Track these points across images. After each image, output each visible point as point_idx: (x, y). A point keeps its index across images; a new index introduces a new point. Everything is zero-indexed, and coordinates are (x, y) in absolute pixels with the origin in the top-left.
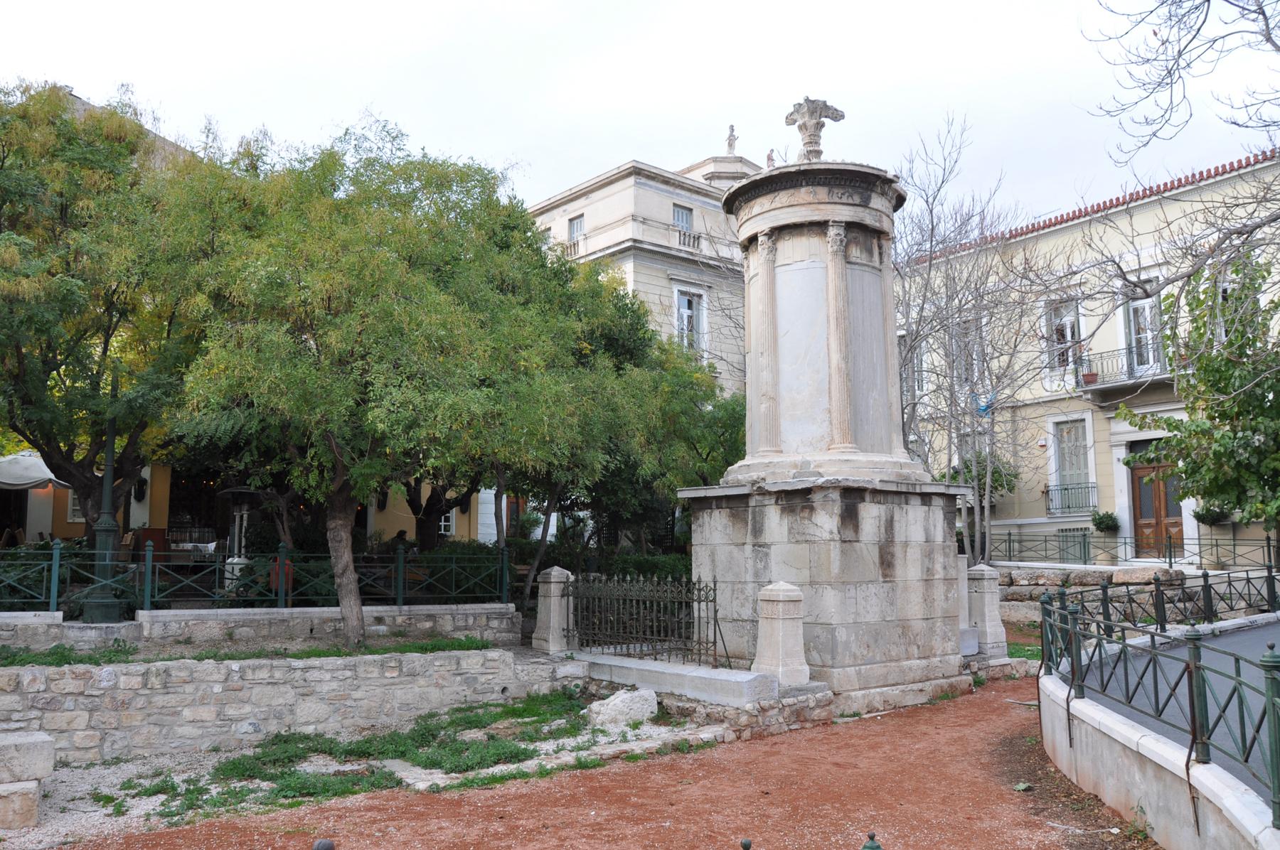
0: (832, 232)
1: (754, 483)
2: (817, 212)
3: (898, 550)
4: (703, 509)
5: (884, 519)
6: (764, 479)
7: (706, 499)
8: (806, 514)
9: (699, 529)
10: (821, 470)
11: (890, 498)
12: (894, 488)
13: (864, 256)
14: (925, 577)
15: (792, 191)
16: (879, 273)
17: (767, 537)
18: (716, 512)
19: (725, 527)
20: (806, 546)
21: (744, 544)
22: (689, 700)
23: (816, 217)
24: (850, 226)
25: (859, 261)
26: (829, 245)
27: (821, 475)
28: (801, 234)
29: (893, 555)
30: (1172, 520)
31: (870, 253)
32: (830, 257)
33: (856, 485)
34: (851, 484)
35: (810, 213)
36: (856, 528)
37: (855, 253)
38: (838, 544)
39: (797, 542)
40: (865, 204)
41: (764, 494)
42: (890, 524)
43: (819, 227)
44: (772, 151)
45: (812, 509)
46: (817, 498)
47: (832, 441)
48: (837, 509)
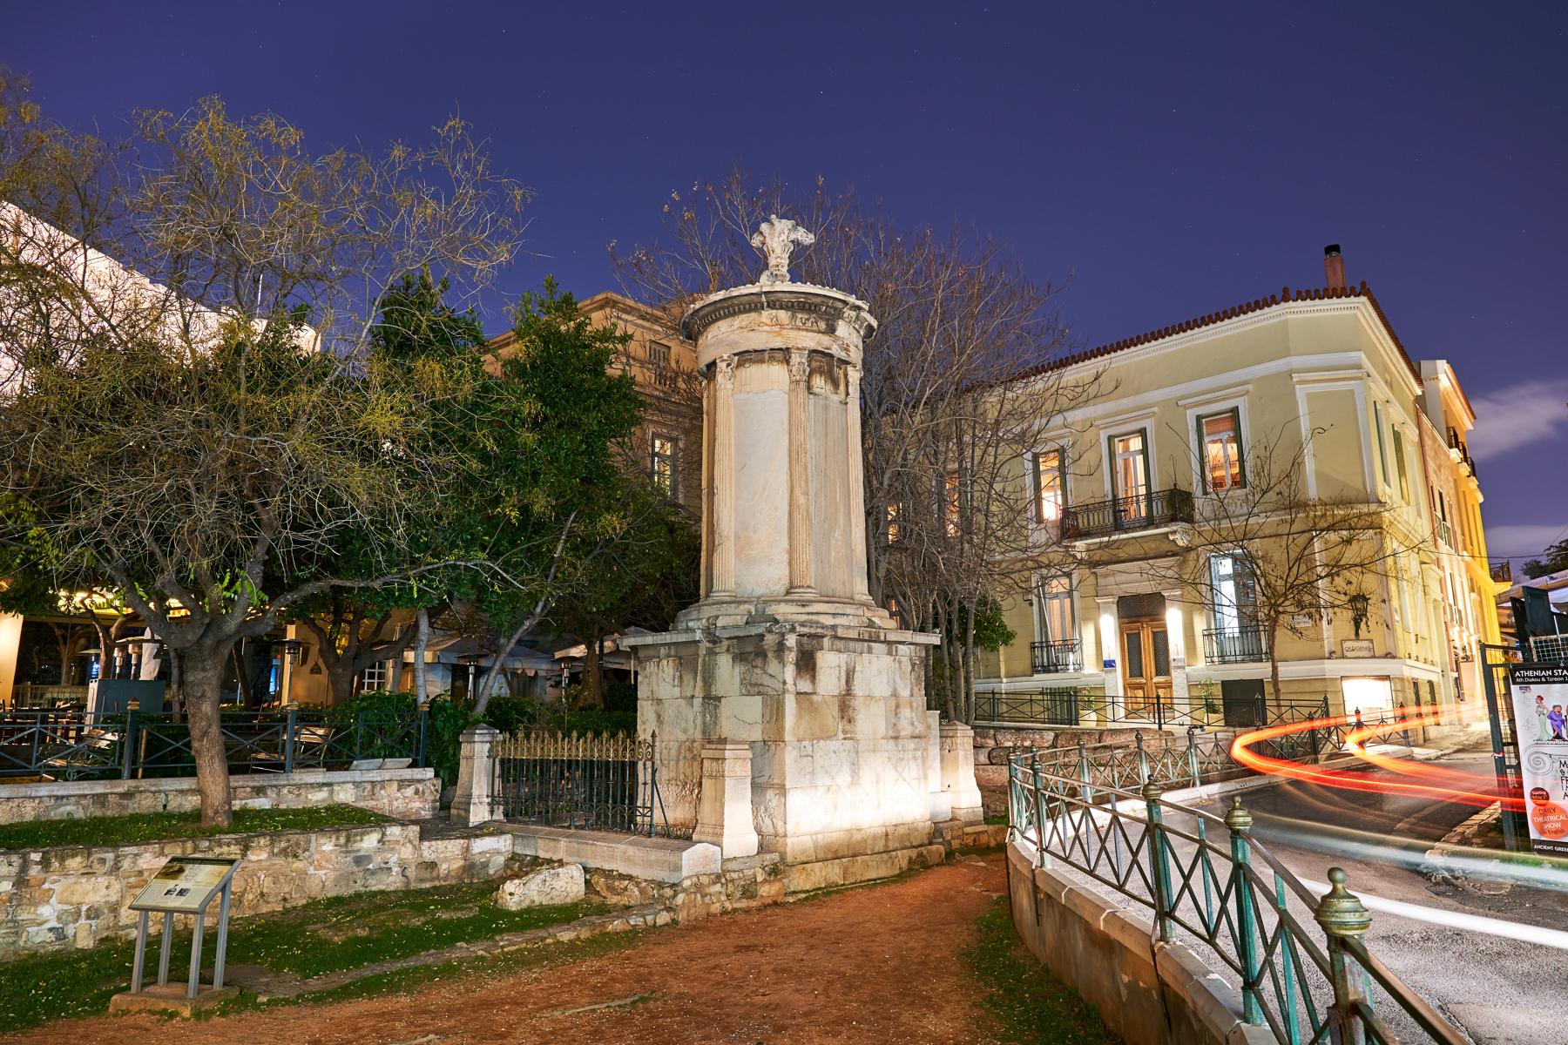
0: (795, 358)
3: (857, 703)
5: (844, 668)
8: (759, 662)
9: (646, 681)
11: (852, 644)
13: (829, 387)
14: (891, 733)
15: (753, 315)
17: (718, 689)
21: (693, 697)
23: (778, 343)
28: (762, 361)
31: (836, 384)
36: (813, 679)
37: (819, 382)
43: (783, 355)
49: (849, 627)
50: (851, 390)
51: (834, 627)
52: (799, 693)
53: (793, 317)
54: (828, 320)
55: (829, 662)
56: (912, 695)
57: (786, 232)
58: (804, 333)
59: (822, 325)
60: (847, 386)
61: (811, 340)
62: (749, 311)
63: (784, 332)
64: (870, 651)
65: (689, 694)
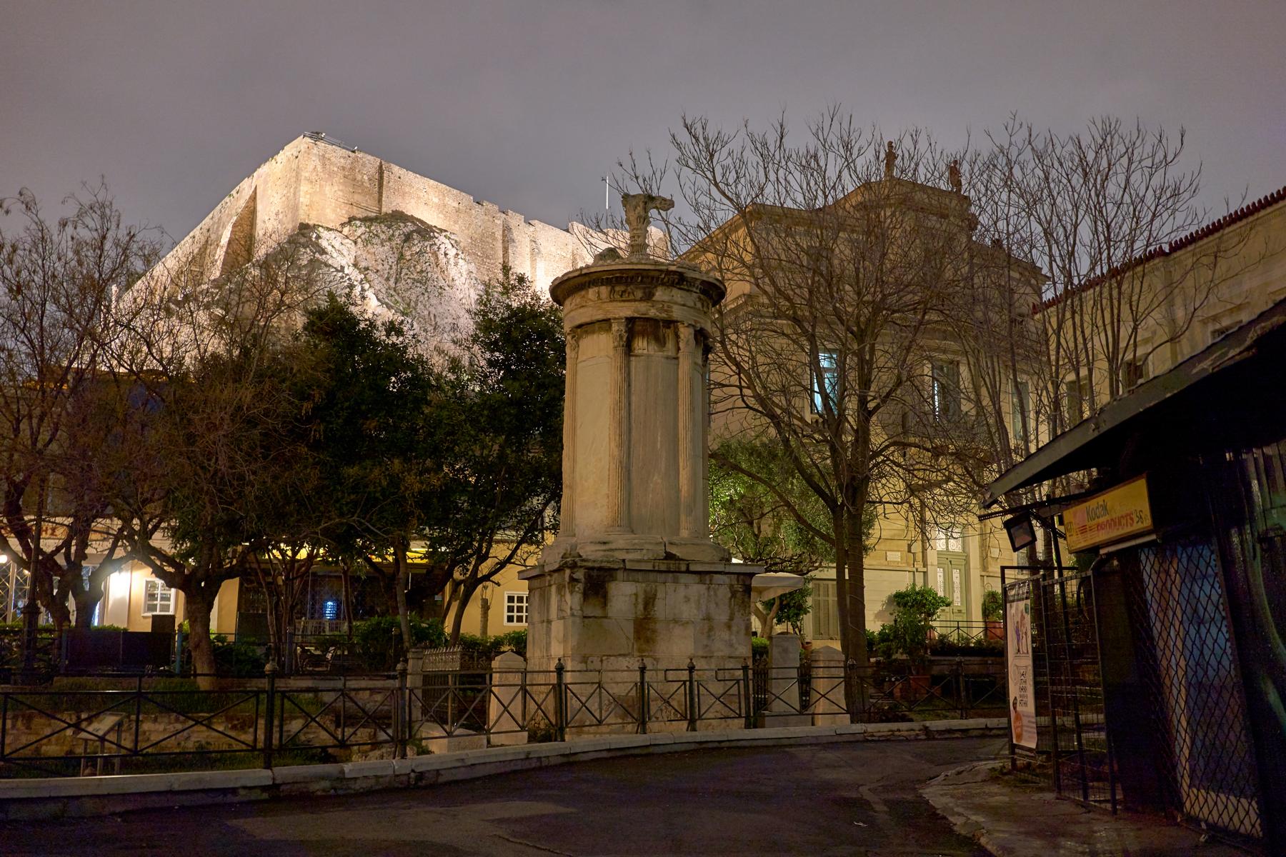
0: (615, 327)
2: (600, 312)
11: (652, 576)
12: (650, 567)
14: (700, 653)
16: (674, 361)
24: (630, 321)
25: (645, 352)
28: (593, 332)
29: (654, 631)
31: (661, 342)
33: (596, 565)
34: (590, 564)
37: (641, 345)
38: (578, 620)
40: (648, 297)
42: (649, 601)
43: (605, 324)
48: (580, 586)
49: (639, 561)
50: (681, 345)
51: (624, 561)
52: (585, 617)
53: (612, 291)
54: (645, 288)
56: (731, 619)
57: (642, 204)
58: (622, 304)
59: (639, 294)
60: (678, 343)
61: (626, 310)
63: (605, 306)
64: (676, 581)
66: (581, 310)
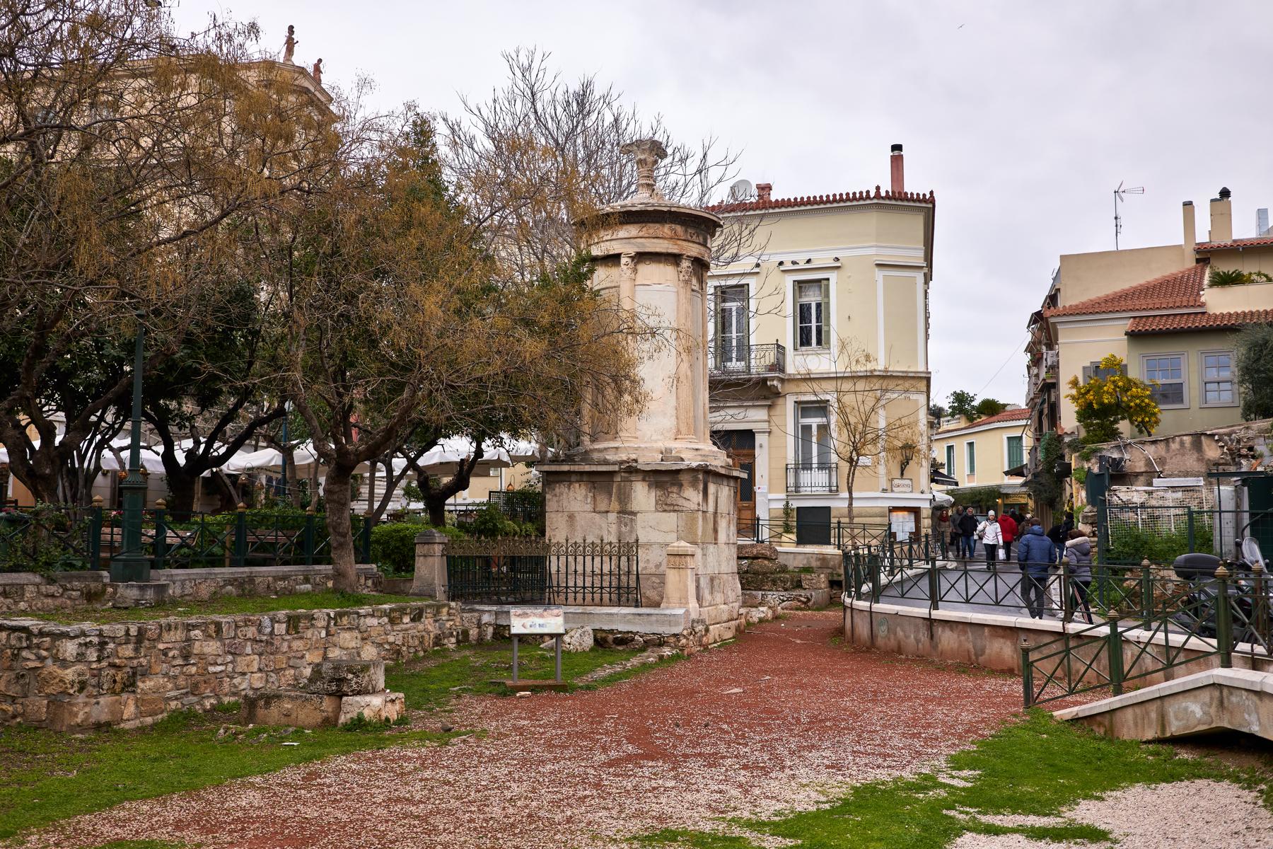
0: (685, 264)
1: (622, 463)
3: (719, 519)
4: (562, 481)
6: (636, 461)
7: (569, 472)
8: (675, 489)
9: (555, 499)
10: (683, 456)
15: (658, 225)
17: (634, 507)
18: (577, 485)
19: (586, 497)
20: (673, 515)
21: (607, 512)
22: (620, 632)
23: (673, 249)
26: (681, 275)
27: (682, 460)
28: (660, 262)
30: (745, 504)
32: (682, 285)
35: (671, 246)
37: (694, 281)
39: (665, 511)
41: (630, 472)
44: (320, 61)
45: (681, 486)
46: (685, 478)
47: (679, 432)
53: (686, 231)
55: (712, 488)
58: (691, 244)
59: (701, 240)
61: (694, 250)
62: (653, 222)
65: (603, 509)
66: (655, 240)
